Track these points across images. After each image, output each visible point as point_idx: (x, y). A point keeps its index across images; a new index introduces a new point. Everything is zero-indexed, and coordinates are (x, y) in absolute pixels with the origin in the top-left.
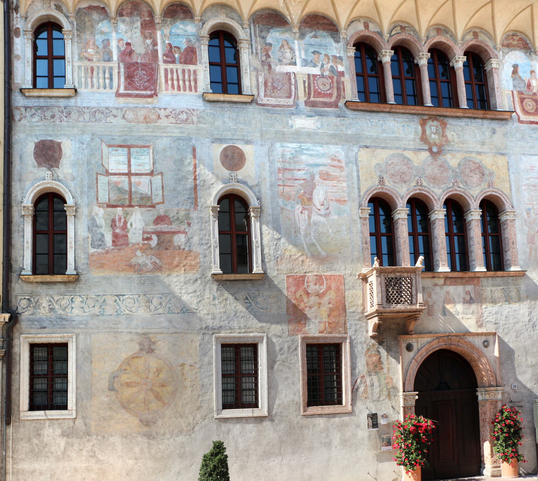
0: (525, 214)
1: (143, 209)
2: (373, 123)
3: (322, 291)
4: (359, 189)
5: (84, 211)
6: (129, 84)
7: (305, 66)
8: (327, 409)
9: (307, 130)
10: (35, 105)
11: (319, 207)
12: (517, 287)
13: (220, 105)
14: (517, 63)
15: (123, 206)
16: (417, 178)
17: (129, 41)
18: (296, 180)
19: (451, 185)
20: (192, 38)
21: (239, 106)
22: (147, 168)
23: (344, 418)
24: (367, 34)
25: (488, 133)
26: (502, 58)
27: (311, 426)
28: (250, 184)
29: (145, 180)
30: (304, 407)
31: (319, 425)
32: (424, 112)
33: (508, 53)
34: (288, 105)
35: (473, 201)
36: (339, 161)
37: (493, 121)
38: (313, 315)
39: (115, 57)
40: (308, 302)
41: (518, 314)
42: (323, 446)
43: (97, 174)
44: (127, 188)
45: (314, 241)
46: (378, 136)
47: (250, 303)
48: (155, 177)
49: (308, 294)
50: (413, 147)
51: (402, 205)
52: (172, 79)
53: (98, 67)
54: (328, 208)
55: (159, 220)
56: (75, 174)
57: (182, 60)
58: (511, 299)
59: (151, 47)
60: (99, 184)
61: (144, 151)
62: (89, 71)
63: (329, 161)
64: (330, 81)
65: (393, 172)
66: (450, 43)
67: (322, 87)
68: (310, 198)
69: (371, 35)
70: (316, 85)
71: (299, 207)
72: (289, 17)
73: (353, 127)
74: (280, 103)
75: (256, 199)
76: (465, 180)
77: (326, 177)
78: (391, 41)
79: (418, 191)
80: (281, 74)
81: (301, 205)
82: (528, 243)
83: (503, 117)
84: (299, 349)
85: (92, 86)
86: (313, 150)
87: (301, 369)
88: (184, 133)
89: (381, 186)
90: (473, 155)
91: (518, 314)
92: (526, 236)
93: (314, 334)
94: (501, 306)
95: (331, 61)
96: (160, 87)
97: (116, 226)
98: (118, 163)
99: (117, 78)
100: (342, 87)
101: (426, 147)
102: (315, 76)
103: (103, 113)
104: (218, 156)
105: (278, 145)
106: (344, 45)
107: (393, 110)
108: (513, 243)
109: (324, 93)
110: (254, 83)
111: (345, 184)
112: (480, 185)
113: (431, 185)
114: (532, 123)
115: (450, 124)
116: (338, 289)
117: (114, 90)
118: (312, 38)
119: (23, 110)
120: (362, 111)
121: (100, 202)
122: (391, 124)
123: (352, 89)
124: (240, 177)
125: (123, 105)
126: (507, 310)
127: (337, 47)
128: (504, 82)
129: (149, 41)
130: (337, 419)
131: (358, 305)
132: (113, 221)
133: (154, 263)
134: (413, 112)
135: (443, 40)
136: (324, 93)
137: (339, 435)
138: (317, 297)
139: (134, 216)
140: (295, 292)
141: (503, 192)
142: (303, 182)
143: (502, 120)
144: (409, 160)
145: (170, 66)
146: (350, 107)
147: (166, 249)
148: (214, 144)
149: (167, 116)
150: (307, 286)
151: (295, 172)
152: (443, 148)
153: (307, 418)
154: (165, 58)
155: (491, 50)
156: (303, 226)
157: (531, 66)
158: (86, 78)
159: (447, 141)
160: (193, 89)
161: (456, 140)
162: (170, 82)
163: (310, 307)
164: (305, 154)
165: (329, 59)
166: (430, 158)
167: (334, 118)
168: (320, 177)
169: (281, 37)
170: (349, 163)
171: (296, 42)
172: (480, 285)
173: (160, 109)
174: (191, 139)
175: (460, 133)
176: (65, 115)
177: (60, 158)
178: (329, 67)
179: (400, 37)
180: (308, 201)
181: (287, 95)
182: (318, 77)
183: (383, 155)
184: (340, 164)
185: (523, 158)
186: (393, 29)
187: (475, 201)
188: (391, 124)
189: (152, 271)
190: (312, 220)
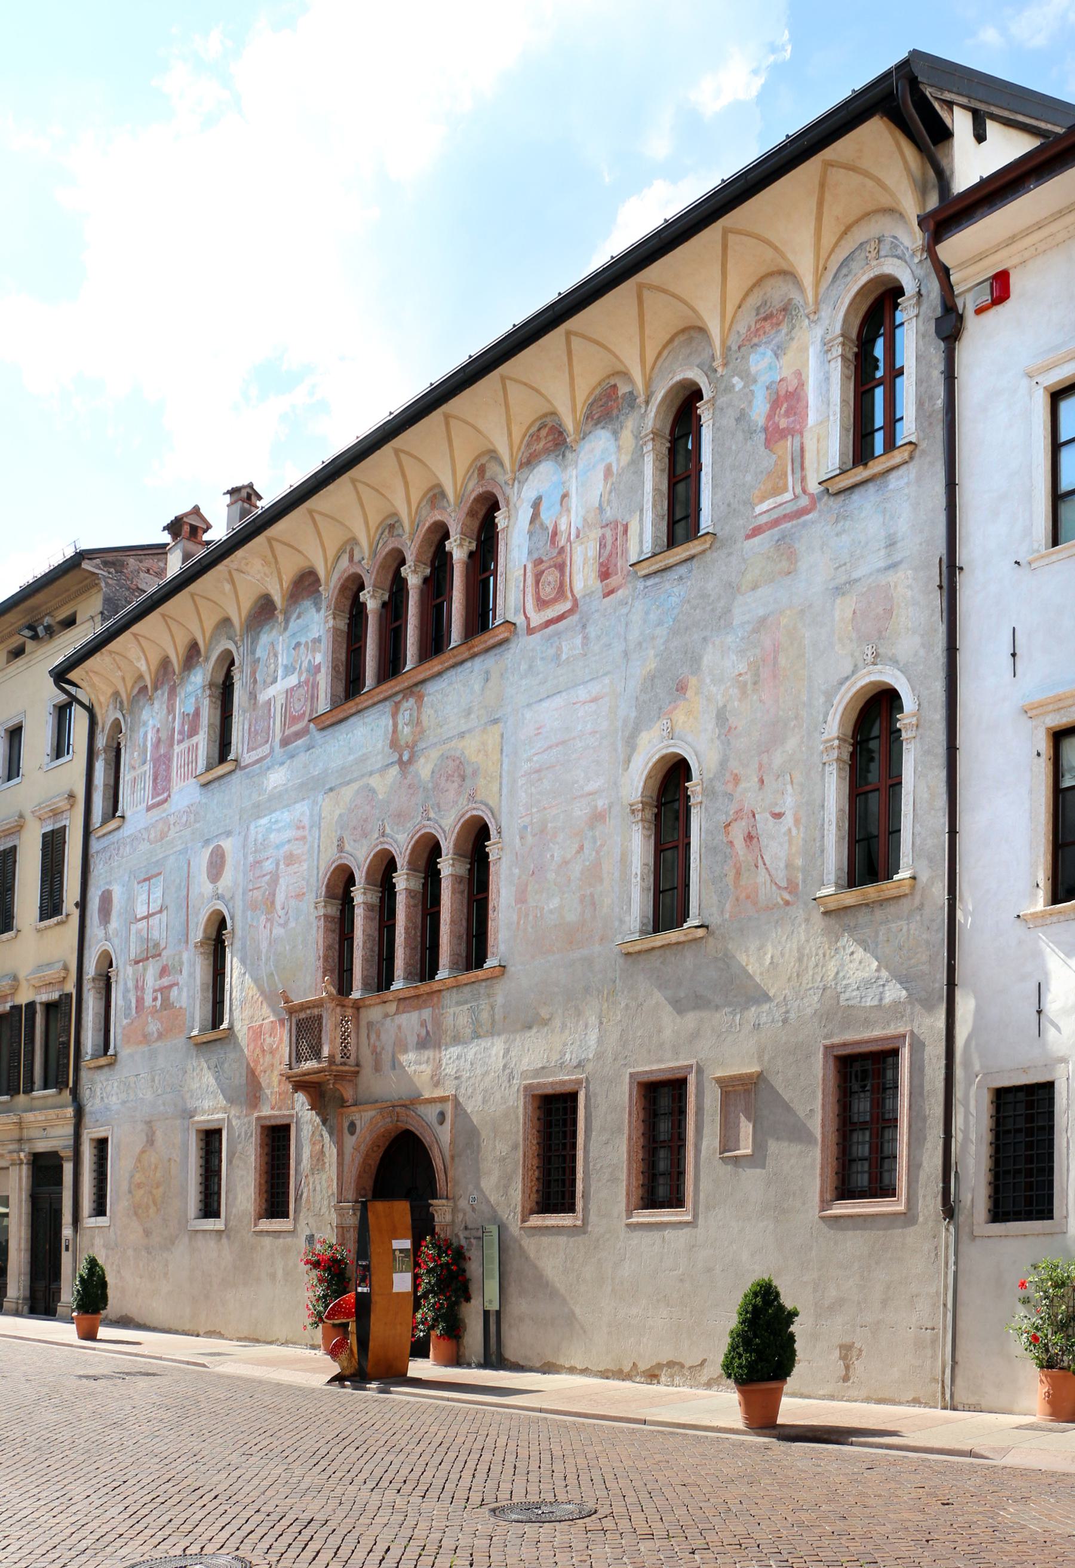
4: (318, 868)
50: (379, 766)
74: (260, 756)
82: (516, 903)
90: (453, 743)
92: (514, 889)
102: (292, 689)
107: (360, 707)
134: (382, 696)
185: (528, 715)
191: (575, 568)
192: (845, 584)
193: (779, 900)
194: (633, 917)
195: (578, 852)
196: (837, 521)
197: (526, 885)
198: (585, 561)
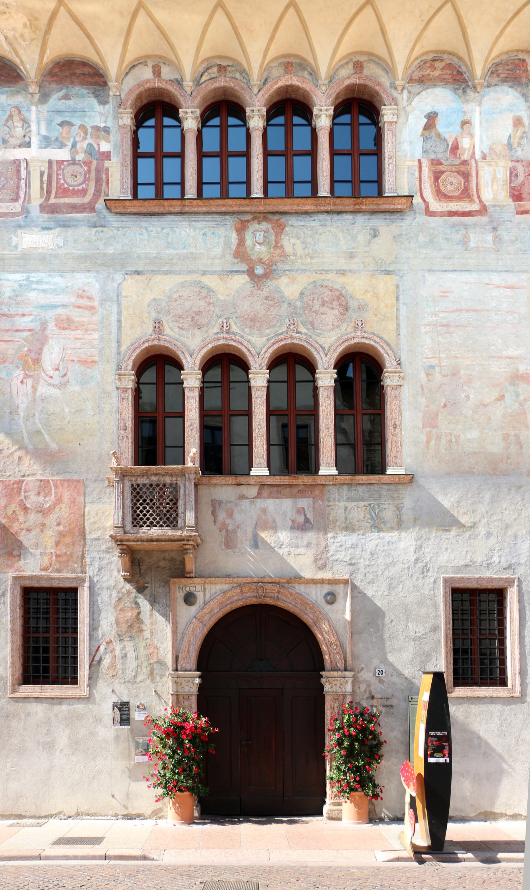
0: (423, 375)
3: (48, 505)
4: (118, 341)
8: (49, 691)
9: (40, 251)
11: (51, 373)
12: (397, 502)
14: (436, 109)
16: (221, 320)
18: (17, 331)
19: (284, 329)
23: (76, 706)
24: (157, 84)
25: (362, 238)
26: (405, 103)
27: (23, 716)
30: (13, 685)
31: (36, 714)
32: (242, 209)
33: (419, 93)
34: (14, 213)
35: (322, 355)
36: (90, 298)
37: (374, 216)
38: (32, 541)
40: (25, 522)
41: (396, 549)
42: (41, 748)
45: (40, 426)
46: (158, 253)
51: (190, 365)
54: (65, 375)
58: (384, 522)
63: (73, 299)
64: (86, 168)
65: (179, 311)
66: (307, 86)
68: (37, 359)
69: (163, 85)
70: (61, 177)
71: (19, 374)
72: (22, 68)
73: (118, 242)
76: (310, 319)
78: (198, 94)
79: (221, 342)
81: (24, 370)
82: (424, 426)
83: (392, 207)
84: (9, 594)
86: (47, 283)
87: (9, 626)
89: (156, 336)
90: (330, 276)
91: (396, 549)
92: (421, 414)
93: (33, 571)
94: (363, 535)
100: (104, 177)
102: (60, 163)
106: (114, 107)
107: (187, 209)
109: (74, 189)
111: (96, 335)
112: (338, 327)
113: (247, 330)
114: (452, 214)
115: (292, 226)
118: (60, 100)
120: (135, 214)
122: (183, 233)
126: (374, 543)
127: (102, 111)
128: (406, 146)
130: (64, 707)
131: (105, 529)
134: (223, 209)
135: (295, 81)
136: (74, 189)
137: (67, 731)
138: (40, 515)
140: (6, 507)
141: (381, 338)
142: (28, 333)
143: (392, 212)
144: (210, 290)
150: (25, 497)
151: (17, 318)
152: (274, 267)
153: (16, 702)
155: (385, 91)
157: (464, 112)
159: (284, 255)
161: (300, 251)
163: (28, 530)
164: (34, 289)
165: (86, 133)
166: (249, 286)
167: (86, 229)
168: (56, 325)
169: (10, 102)
170: (106, 300)
171: (34, 108)
172: (325, 498)
175: (309, 240)
179: (216, 85)
180: (34, 364)
181: (13, 196)
184: (90, 304)
185: (430, 278)
186: (205, 72)
187: (326, 355)
188: (183, 233)
190: (38, 393)
195: (498, 400)
197: (437, 415)
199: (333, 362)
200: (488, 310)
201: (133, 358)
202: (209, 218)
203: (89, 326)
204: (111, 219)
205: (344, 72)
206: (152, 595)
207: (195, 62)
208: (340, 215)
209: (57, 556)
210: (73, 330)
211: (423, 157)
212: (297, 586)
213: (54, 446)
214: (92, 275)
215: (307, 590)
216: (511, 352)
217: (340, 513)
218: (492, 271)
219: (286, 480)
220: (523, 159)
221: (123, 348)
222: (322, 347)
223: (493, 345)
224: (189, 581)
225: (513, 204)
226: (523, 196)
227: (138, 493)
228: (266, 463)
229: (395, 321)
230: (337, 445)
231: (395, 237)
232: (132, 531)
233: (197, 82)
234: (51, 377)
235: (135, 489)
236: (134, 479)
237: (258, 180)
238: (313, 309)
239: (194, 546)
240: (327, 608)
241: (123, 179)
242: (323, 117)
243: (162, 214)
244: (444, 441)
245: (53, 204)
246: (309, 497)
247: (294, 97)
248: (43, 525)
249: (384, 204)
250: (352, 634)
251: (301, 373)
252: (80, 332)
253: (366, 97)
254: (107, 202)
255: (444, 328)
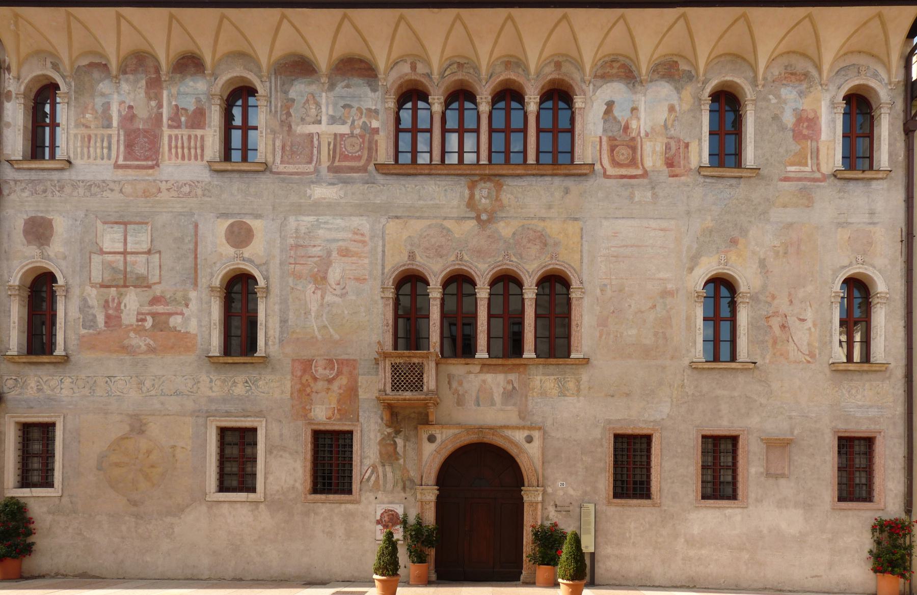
0: (598, 290)
1: (138, 290)
2: (408, 189)
3: (332, 376)
4: (383, 266)
5: (75, 292)
6: (129, 153)
7: (332, 124)
9: (327, 200)
10: (25, 178)
11: (334, 287)
12: (577, 377)
13: (227, 175)
15: (117, 286)
16: (457, 251)
17: (132, 104)
18: (310, 257)
19: (501, 259)
20: (202, 97)
21: (250, 175)
22: (145, 247)
24: (414, 77)
25: (558, 194)
28: (257, 261)
29: (142, 259)
32: (473, 172)
35: (527, 276)
36: (362, 235)
37: (567, 178)
39: (115, 123)
43: (90, 253)
44: (122, 268)
47: (250, 386)
48: (152, 256)
49: (315, 379)
52: (176, 147)
53: (96, 135)
54: (344, 288)
55: (155, 300)
56: (67, 253)
57: (189, 125)
58: (568, 390)
59: (155, 110)
60: (92, 264)
61: (142, 228)
62: (86, 139)
63: (350, 236)
64: (361, 140)
66: (521, 80)
67: (349, 149)
68: (324, 277)
70: (343, 146)
71: (311, 287)
74: (299, 170)
75: (262, 279)
77: (345, 253)
79: (457, 267)
80: (300, 135)
83: (580, 172)
85: (89, 157)
86: (332, 224)
88: (185, 208)
90: (535, 222)
95: (363, 116)
96: (162, 156)
97: (109, 306)
98: (113, 241)
99: (116, 147)
101: (473, 215)
103: (99, 187)
104: (223, 232)
105: (292, 219)
107: (433, 172)
108: (577, 325)
110: (270, 148)
111: (366, 261)
116: (351, 373)
117: (113, 161)
119: (12, 183)
121: (92, 282)
122: (430, 189)
123: (387, 149)
124: (246, 255)
125: (121, 177)
128: (590, 127)
129: (153, 103)
132: (107, 302)
133: (148, 345)
134: (459, 172)
135: (513, 76)
139: (128, 296)
140: (301, 377)
142: (318, 259)
143: (580, 175)
144: (449, 230)
145: (176, 132)
146: (380, 171)
147: (161, 331)
148: (219, 220)
149: (168, 190)
152: (495, 215)
154: (170, 122)
156: (314, 307)
158: (82, 147)
159: (502, 207)
160: (199, 157)
162: (173, 151)
164: (322, 228)
166: (476, 228)
168: (338, 253)
170: (374, 236)
173: (161, 182)
174: (193, 214)
176: (58, 189)
177: (52, 236)
178: (361, 124)
182: (346, 136)
183: (417, 226)
185: (605, 223)
187: (530, 277)
188: (430, 189)
189: (145, 353)
190: (325, 300)
191: (645, 153)
192: (844, 223)
193: (803, 359)
194: (697, 350)
195: (651, 308)
196: (839, 192)
198: (654, 152)
199: (535, 281)
200: (647, 246)
201: (393, 277)
202: (449, 178)
203: (362, 254)
204: (379, 178)
205: (549, 69)
206: (405, 436)
207: (440, 61)
208: (542, 178)
209: (339, 410)
210: (351, 257)
211: (603, 135)
212: (506, 431)
213: (337, 337)
214: (365, 218)
215: (513, 434)
216: (662, 275)
217: (538, 383)
218: (650, 218)
219: (500, 361)
220: (675, 136)
221: (386, 270)
222: (527, 272)
223: (649, 271)
224: (431, 427)
225: (667, 169)
226: (674, 164)
227: (396, 369)
228: (486, 350)
229: (580, 253)
230: (536, 337)
231: (581, 194)
232: (391, 394)
233: (442, 76)
234: (335, 290)
235: (393, 366)
236: (392, 359)
237: (484, 151)
238: (522, 245)
239: (434, 404)
240: (527, 446)
241: (388, 148)
242: (532, 104)
243: (415, 175)
244: (612, 336)
245: (337, 166)
246: (515, 373)
247: (512, 87)
248: (328, 389)
249: (573, 169)
250: (543, 463)
251: (513, 288)
252: (354, 258)
253: (563, 88)
254: (376, 166)
255: (614, 259)
